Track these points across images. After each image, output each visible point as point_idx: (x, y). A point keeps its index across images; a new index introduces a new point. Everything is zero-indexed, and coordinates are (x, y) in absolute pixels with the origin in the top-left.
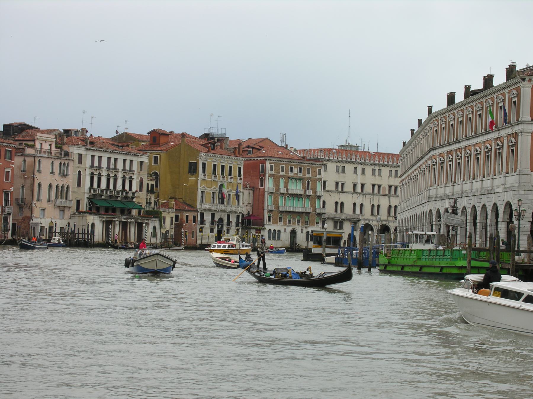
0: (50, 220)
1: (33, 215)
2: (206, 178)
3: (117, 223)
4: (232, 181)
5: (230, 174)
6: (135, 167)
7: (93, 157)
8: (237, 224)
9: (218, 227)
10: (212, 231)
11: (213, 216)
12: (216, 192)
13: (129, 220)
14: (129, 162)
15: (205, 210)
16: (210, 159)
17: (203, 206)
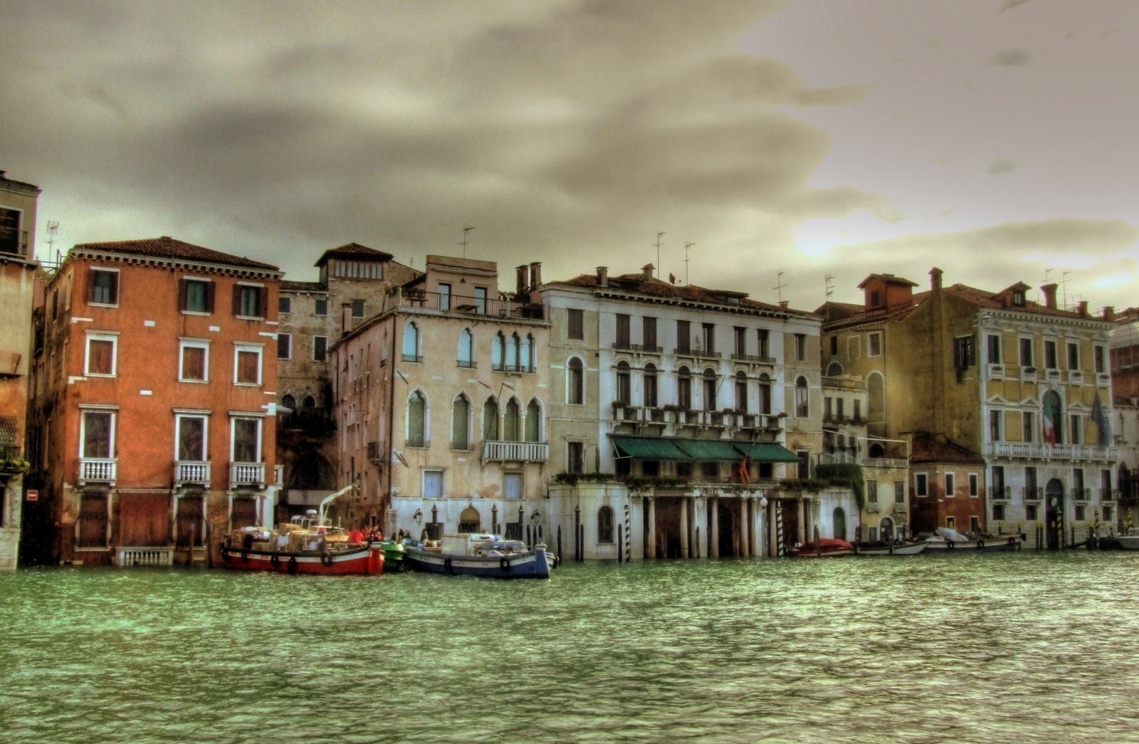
0: (464, 504)
1: (393, 489)
2: (1002, 376)
3: (700, 505)
4: (1081, 381)
5: (1074, 364)
6: (776, 347)
7: (623, 320)
8: (1107, 494)
9: (1049, 502)
10: (1031, 513)
11: (1031, 473)
12: (1036, 412)
13: (745, 495)
14: (756, 334)
15: (1004, 458)
16: (1010, 326)
17: (999, 449)
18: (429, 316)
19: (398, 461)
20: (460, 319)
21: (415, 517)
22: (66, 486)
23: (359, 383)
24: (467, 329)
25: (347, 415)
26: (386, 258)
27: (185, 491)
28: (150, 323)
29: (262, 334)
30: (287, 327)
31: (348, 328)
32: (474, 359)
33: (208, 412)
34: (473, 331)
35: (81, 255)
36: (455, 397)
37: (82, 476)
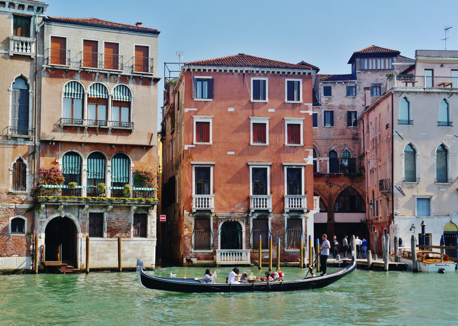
0: (447, 220)
18: (416, 92)
19: (398, 192)
20: (439, 93)
21: (411, 230)
22: (186, 212)
23: (375, 140)
24: (445, 100)
25: (370, 163)
26: (394, 54)
27: (257, 215)
28: (231, 110)
29: (301, 112)
30: (331, 106)
31: (369, 104)
32: (450, 121)
33: (270, 164)
34: (449, 100)
35: (189, 70)
36: (437, 147)
37: (194, 206)
